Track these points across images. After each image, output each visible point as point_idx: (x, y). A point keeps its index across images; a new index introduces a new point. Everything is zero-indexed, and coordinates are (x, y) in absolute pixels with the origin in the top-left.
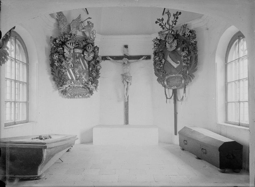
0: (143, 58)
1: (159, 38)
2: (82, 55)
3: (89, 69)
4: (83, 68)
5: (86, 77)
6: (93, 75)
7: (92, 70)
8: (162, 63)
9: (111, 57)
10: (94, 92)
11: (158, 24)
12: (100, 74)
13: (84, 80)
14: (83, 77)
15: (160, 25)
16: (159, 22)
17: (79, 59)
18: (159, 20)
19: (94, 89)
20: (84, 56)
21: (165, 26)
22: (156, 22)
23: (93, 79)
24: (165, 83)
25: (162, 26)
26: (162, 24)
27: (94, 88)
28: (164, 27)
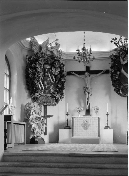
0: (102, 72)
1: (114, 54)
2: (50, 70)
3: (56, 82)
4: (51, 81)
5: (53, 89)
6: (59, 87)
7: (58, 83)
8: (117, 75)
9: (75, 72)
10: (59, 101)
11: (113, 42)
12: (65, 86)
13: (51, 91)
14: (51, 88)
15: (115, 43)
16: (113, 41)
17: (48, 74)
18: (113, 39)
19: (60, 98)
20: (52, 71)
21: (118, 44)
22: (111, 42)
23: (59, 90)
24: (121, 92)
25: (116, 44)
26: (116, 43)
27: (59, 97)
28: (117, 44)
